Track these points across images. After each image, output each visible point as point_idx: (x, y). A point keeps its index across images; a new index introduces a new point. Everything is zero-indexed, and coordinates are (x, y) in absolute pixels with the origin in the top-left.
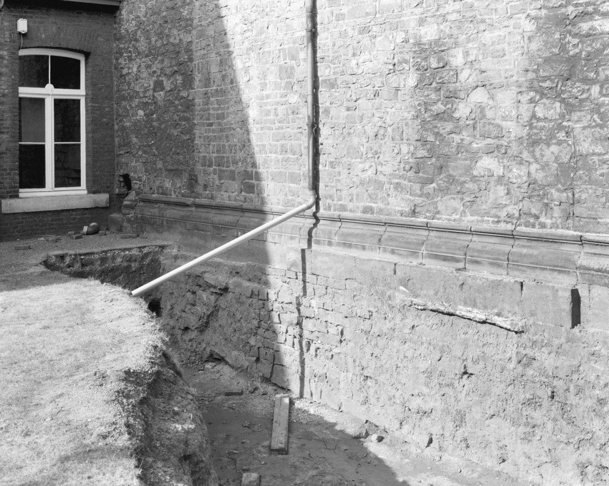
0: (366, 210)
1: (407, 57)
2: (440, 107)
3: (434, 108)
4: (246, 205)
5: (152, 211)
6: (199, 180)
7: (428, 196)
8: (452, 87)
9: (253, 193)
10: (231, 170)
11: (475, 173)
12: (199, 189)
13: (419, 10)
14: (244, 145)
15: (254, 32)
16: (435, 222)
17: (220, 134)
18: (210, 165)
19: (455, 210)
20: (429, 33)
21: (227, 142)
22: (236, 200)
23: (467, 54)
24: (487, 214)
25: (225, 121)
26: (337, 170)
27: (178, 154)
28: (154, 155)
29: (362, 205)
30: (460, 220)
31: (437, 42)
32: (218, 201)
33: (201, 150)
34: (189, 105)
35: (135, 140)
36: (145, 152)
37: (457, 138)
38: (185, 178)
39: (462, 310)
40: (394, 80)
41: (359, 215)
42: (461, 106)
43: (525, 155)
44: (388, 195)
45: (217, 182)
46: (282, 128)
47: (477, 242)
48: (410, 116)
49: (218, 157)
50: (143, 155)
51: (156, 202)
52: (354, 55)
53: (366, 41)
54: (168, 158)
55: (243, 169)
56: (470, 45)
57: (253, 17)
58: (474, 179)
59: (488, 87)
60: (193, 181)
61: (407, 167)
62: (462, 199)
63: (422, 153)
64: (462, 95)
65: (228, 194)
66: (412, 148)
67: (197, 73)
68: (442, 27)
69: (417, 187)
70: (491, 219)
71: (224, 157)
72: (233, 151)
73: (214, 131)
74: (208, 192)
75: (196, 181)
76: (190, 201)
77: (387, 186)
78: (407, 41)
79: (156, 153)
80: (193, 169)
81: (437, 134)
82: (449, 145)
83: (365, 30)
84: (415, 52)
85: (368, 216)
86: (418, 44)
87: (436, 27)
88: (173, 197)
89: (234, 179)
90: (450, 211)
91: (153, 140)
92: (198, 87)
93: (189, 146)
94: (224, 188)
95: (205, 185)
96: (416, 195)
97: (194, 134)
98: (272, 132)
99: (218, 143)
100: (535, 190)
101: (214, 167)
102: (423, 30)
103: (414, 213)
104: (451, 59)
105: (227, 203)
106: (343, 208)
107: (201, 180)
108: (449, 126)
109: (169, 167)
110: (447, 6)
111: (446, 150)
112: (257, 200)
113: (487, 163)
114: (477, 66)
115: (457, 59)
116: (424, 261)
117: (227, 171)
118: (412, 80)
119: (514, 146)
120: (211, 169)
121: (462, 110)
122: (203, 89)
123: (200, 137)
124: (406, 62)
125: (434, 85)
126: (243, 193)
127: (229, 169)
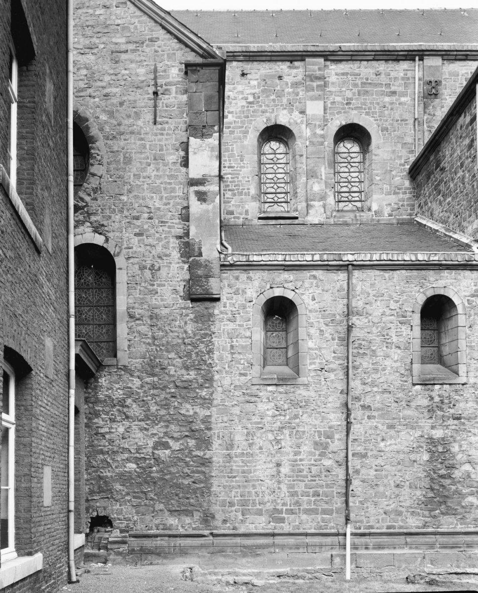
0: (389, 527)
1: (422, 445)
2: (443, 472)
3: (440, 472)
4: (276, 531)
5: (148, 543)
6: (217, 516)
7: (435, 517)
8: (451, 462)
9: (284, 523)
10: (258, 509)
11: (463, 504)
12: (218, 523)
13: (430, 421)
14: (274, 492)
15: (288, 417)
16: (439, 530)
17: (245, 484)
18: (231, 504)
19: (452, 524)
20: (438, 434)
21: (254, 489)
22: (263, 528)
23: (461, 446)
25: (252, 474)
26: (365, 505)
27: (188, 498)
28: (152, 499)
29: (385, 525)
30: (455, 528)
31: (443, 439)
32: (242, 530)
33: (219, 495)
34: (206, 462)
35: (118, 487)
36: (134, 497)
38: (197, 516)
39: (469, 570)
40: (413, 457)
41: (384, 530)
42: (456, 471)
44: (406, 518)
45: (241, 517)
46: (315, 481)
48: (423, 476)
49: (241, 500)
50: (133, 500)
51: (156, 536)
52: (383, 440)
53: (392, 432)
54: (172, 501)
55: (272, 507)
56: (463, 442)
57: (286, 406)
58: (463, 507)
59: (472, 463)
60: (208, 518)
61: (420, 503)
62: (455, 518)
63: (431, 495)
64: (457, 466)
65: (254, 525)
66: (424, 493)
67: (216, 439)
68: (446, 431)
69: (427, 513)
70: (472, 526)
71: (249, 500)
72: (261, 495)
73: (236, 481)
74: (228, 525)
75: (213, 517)
76: (206, 532)
77: (405, 513)
78: (422, 436)
79: (156, 498)
80: (208, 509)
82: (448, 491)
83: (391, 427)
84: (428, 442)
85: (392, 531)
86: (431, 439)
87: (442, 431)
88: (181, 531)
89: (261, 515)
90: (448, 524)
91: (150, 488)
92: (216, 449)
93: (206, 490)
94: (248, 520)
95: (224, 520)
96: (426, 517)
97: (211, 484)
98: (304, 483)
99: (241, 490)
101: (236, 507)
102: (434, 432)
103: (424, 526)
104: (451, 448)
105: (254, 531)
106: (372, 527)
107: (219, 517)
108: (448, 481)
109: (174, 509)
110: (449, 421)
111: (446, 494)
112: (288, 527)
114: (467, 453)
115: (455, 448)
116: (438, 550)
117: (252, 509)
118: (426, 457)
120: (233, 508)
121: (457, 474)
122: (225, 451)
123: (219, 486)
124: (422, 447)
125: (440, 460)
126: (271, 523)
127: (255, 508)
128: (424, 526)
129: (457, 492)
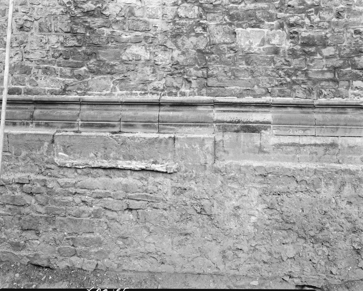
7: (79, 77)
11: (124, 58)
16: (86, 98)
19: (106, 88)
24: (136, 88)
30: (110, 94)
37: (107, 31)
43: (169, 44)
44: (37, 78)
47: (128, 113)
48: (58, 12)
58: (123, 62)
61: (57, 54)
62: (112, 79)
66: (61, 39)
69: (67, 71)
70: (139, 92)
77: (34, 70)
81: (89, 28)
82: (99, 36)
90: (101, 88)
96: (66, 77)
100: (177, 69)
103: (64, 91)
108: (99, 21)
111: (96, 41)
113: (136, 50)
119: (160, 38)
128: (64, 91)
129: (112, 37)
